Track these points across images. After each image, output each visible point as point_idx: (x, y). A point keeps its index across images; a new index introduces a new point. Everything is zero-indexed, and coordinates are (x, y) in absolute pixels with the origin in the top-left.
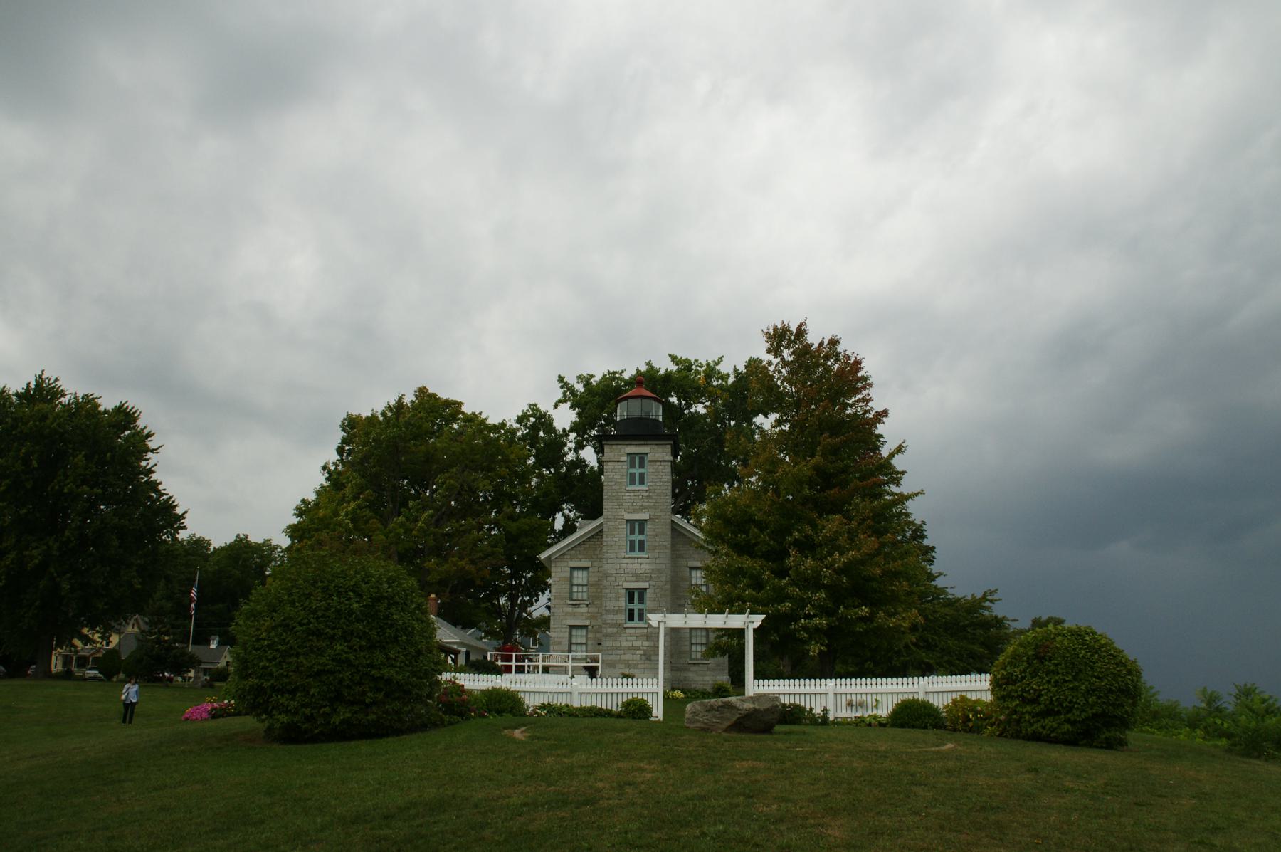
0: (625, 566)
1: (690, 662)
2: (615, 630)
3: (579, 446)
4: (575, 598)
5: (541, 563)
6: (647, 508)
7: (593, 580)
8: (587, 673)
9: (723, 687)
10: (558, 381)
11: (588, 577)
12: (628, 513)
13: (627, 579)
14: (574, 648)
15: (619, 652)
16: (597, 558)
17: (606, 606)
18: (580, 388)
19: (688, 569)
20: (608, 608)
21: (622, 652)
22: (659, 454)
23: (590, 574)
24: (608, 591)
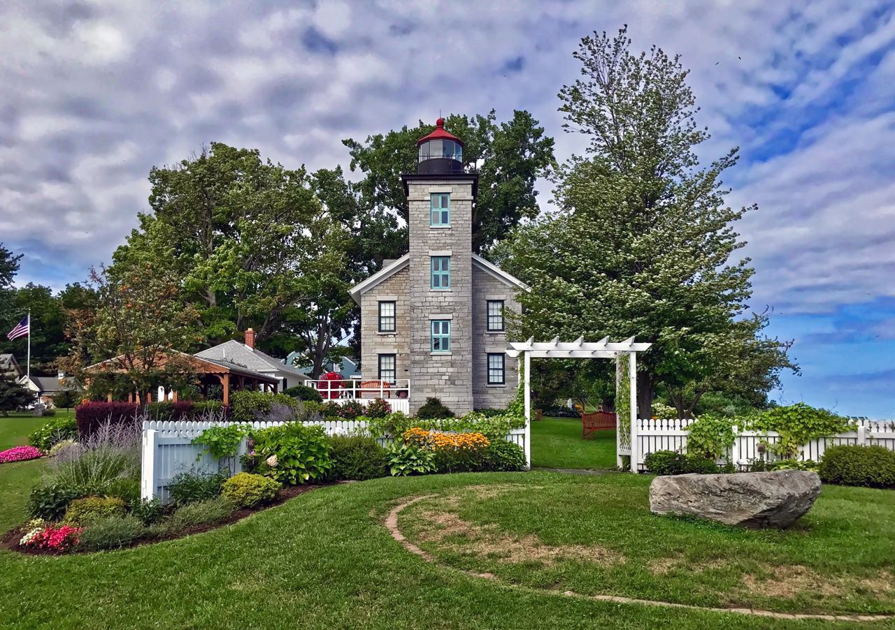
2: (422, 358)
6: (451, 245)
12: (433, 250)
14: (383, 374)
21: (429, 377)
22: (461, 194)
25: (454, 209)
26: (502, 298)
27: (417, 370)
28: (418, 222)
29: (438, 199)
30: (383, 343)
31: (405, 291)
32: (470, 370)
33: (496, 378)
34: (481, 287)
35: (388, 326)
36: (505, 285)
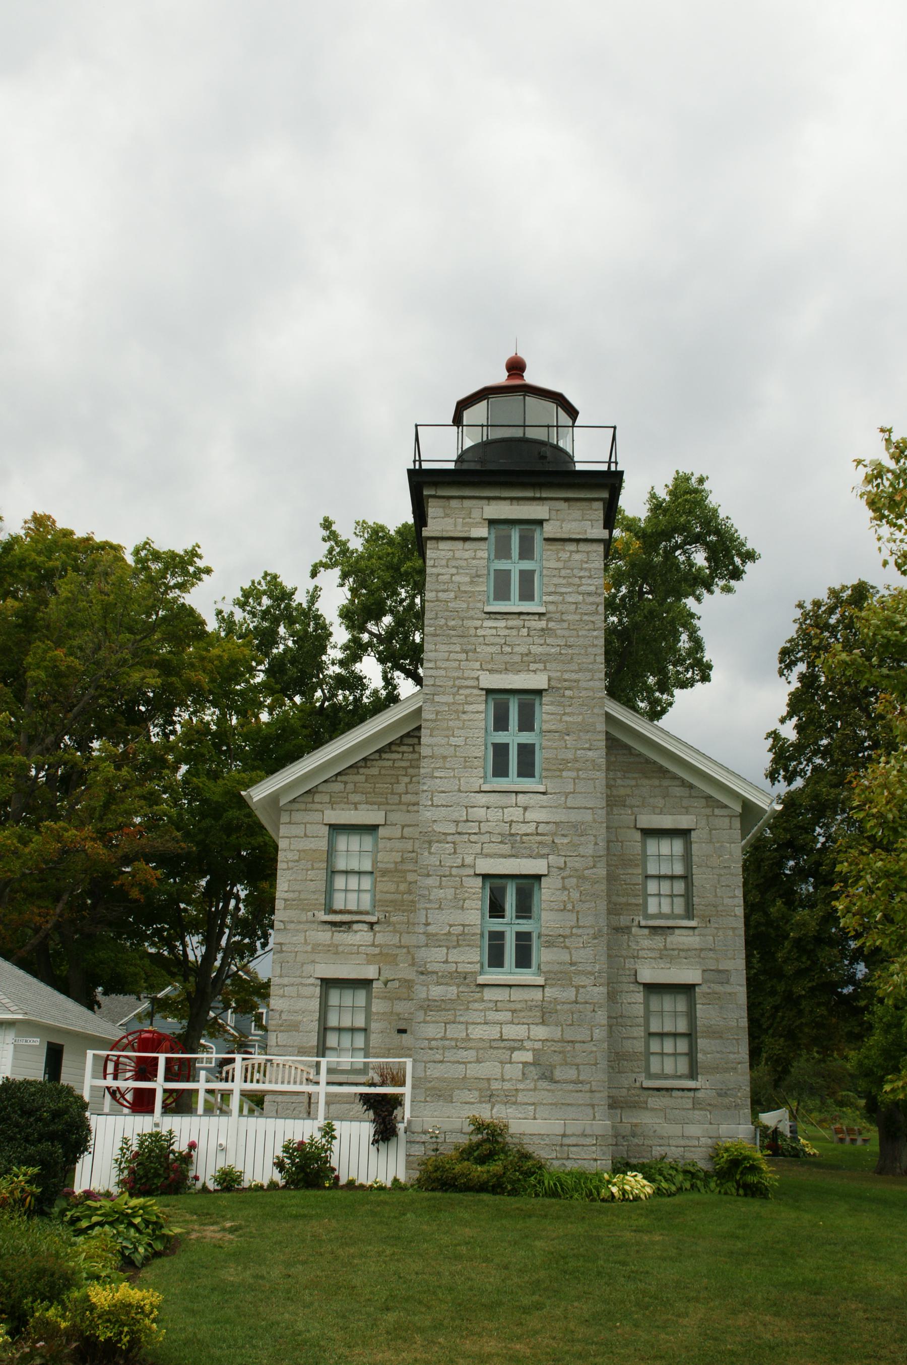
0: (480, 813)
1: (648, 1084)
2: (452, 992)
3: (355, 650)
4: (338, 904)
5: (250, 814)
6: (543, 660)
7: (387, 859)
8: (371, 1112)
9: (746, 1158)
11: (375, 851)
12: (491, 671)
14: (332, 1040)
15: (463, 1054)
16: (400, 803)
17: (427, 924)
19: (638, 836)
20: (431, 929)
21: (471, 1055)
22: (574, 525)
23: (381, 845)
24: (430, 881)
25: (553, 564)
26: (683, 821)
27: (432, 1031)
28: (452, 595)
29: (510, 537)
30: (337, 946)
31: (405, 799)
32: (599, 1034)
33: (669, 1067)
34: (622, 791)
35: (352, 897)
36: (691, 786)
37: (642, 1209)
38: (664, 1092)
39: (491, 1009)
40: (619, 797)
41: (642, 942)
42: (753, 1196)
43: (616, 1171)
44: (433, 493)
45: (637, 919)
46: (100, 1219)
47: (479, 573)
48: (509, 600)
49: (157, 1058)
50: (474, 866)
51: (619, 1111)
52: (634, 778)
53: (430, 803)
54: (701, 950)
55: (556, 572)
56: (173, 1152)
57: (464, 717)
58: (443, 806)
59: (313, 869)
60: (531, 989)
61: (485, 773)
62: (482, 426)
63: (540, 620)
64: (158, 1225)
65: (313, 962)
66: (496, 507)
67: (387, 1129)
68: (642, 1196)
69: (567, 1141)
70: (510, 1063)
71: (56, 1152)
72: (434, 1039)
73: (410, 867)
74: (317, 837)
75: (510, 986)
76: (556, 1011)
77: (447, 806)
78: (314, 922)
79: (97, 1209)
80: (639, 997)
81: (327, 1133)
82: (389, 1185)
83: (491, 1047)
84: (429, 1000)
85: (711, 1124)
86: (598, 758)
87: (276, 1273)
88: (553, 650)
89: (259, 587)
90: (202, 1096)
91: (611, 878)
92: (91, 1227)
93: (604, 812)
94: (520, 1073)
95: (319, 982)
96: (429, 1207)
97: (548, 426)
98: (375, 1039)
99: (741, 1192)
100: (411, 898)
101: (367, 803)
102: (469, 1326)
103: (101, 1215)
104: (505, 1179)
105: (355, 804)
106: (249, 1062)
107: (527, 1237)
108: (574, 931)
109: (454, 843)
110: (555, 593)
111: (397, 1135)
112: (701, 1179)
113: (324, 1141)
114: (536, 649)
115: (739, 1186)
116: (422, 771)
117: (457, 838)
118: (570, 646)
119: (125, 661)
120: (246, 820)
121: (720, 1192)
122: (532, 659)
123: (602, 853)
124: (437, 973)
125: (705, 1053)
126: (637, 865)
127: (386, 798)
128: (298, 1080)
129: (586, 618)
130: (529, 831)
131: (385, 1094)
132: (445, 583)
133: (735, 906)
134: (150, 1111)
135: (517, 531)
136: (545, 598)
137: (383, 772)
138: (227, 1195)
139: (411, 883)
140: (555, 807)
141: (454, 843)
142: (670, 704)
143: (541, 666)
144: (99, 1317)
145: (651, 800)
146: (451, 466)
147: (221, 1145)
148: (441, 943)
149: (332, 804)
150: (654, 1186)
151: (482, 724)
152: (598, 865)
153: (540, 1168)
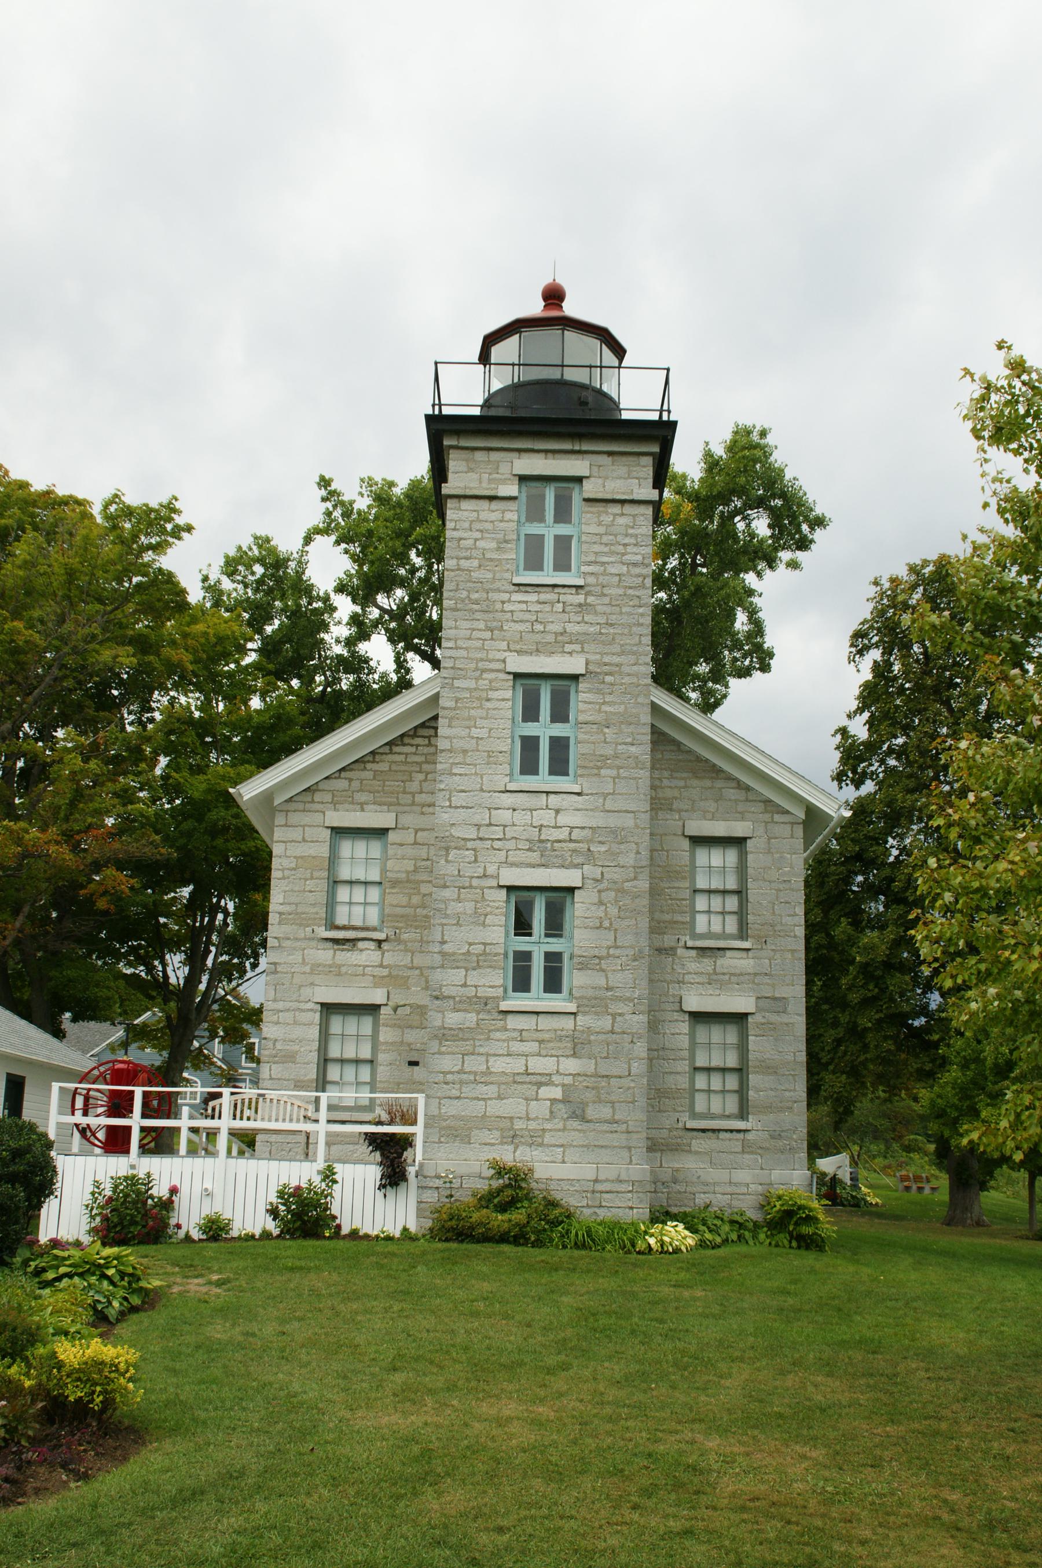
0: (505, 816)
1: (692, 1124)
2: (471, 1019)
3: (362, 629)
4: (341, 920)
5: (239, 814)
6: (581, 640)
7: (398, 867)
8: (378, 1154)
9: (801, 1207)
10: (319, 484)
11: (385, 858)
12: (519, 652)
13: (514, 857)
14: (333, 1073)
16: (413, 804)
17: (443, 942)
18: (363, 503)
19: (686, 844)
20: (447, 948)
21: (492, 1090)
23: (390, 852)
24: (447, 893)
25: (593, 529)
26: (739, 829)
27: (448, 1063)
28: (476, 563)
30: (340, 966)
31: (419, 798)
34: (669, 793)
35: (358, 910)
36: (748, 789)
37: (683, 1262)
38: (710, 1134)
39: (514, 1039)
40: (665, 799)
41: (688, 964)
42: (808, 1248)
43: (654, 1220)
44: (454, 443)
45: (683, 939)
46: (69, 1269)
47: (507, 538)
48: (542, 569)
49: (133, 1092)
50: (497, 877)
51: (658, 1155)
52: (682, 779)
53: (448, 804)
54: (755, 974)
55: (596, 539)
56: (152, 1197)
57: (488, 705)
58: (463, 807)
59: (312, 878)
60: (562, 1016)
61: (512, 770)
62: (513, 365)
63: (578, 594)
64: (135, 1277)
65: (312, 984)
66: (528, 461)
67: (395, 1173)
68: (683, 1248)
69: (599, 1187)
70: (537, 1099)
71: (17, 1196)
72: (452, 1073)
73: (425, 877)
74: (317, 841)
75: (537, 1013)
76: (590, 1042)
77: (467, 808)
78: (313, 939)
79: (65, 1259)
80: (684, 1027)
81: (327, 1177)
82: (397, 1235)
83: (515, 1082)
84: (445, 1028)
85: (762, 1169)
86: (642, 755)
87: (269, 1330)
88: (592, 629)
89: (250, 553)
90: (184, 1135)
91: (654, 892)
92: (59, 1279)
93: (647, 816)
94: (547, 1112)
95: (319, 1007)
96: (443, 1258)
97: (591, 367)
98: (382, 1071)
99: (794, 1244)
100: (425, 912)
101: (374, 803)
102: (486, 1387)
103: (70, 1266)
104: (528, 1229)
105: (362, 804)
106: (239, 1097)
107: (553, 1292)
108: (612, 951)
109: (474, 850)
110: (596, 562)
111: (406, 1180)
112: (749, 1230)
113: (324, 1184)
114: (571, 627)
115: (792, 1237)
116: (439, 767)
117: (478, 844)
118: (611, 625)
119: (94, 637)
120: (234, 822)
121: (770, 1244)
122: (566, 639)
123: (644, 863)
124: (454, 998)
125: (758, 1090)
126: (684, 878)
127: (397, 798)
128: (295, 1117)
129: (630, 592)
130: (561, 837)
131: (394, 1134)
132: (467, 549)
133: (795, 925)
134: (126, 1151)
135: (553, 489)
136: (583, 569)
137: (394, 767)
138: (213, 1245)
139: (425, 895)
140: (592, 810)
141: (474, 850)
142: (725, 696)
143: (578, 647)
144: (68, 1376)
145: (702, 804)
146: (476, 411)
147: (206, 1190)
148: (458, 964)
149: (335, 804)
150: (697, 1237)
151: (509, 713)
152: (640, 877)
153: (568, 1217)
